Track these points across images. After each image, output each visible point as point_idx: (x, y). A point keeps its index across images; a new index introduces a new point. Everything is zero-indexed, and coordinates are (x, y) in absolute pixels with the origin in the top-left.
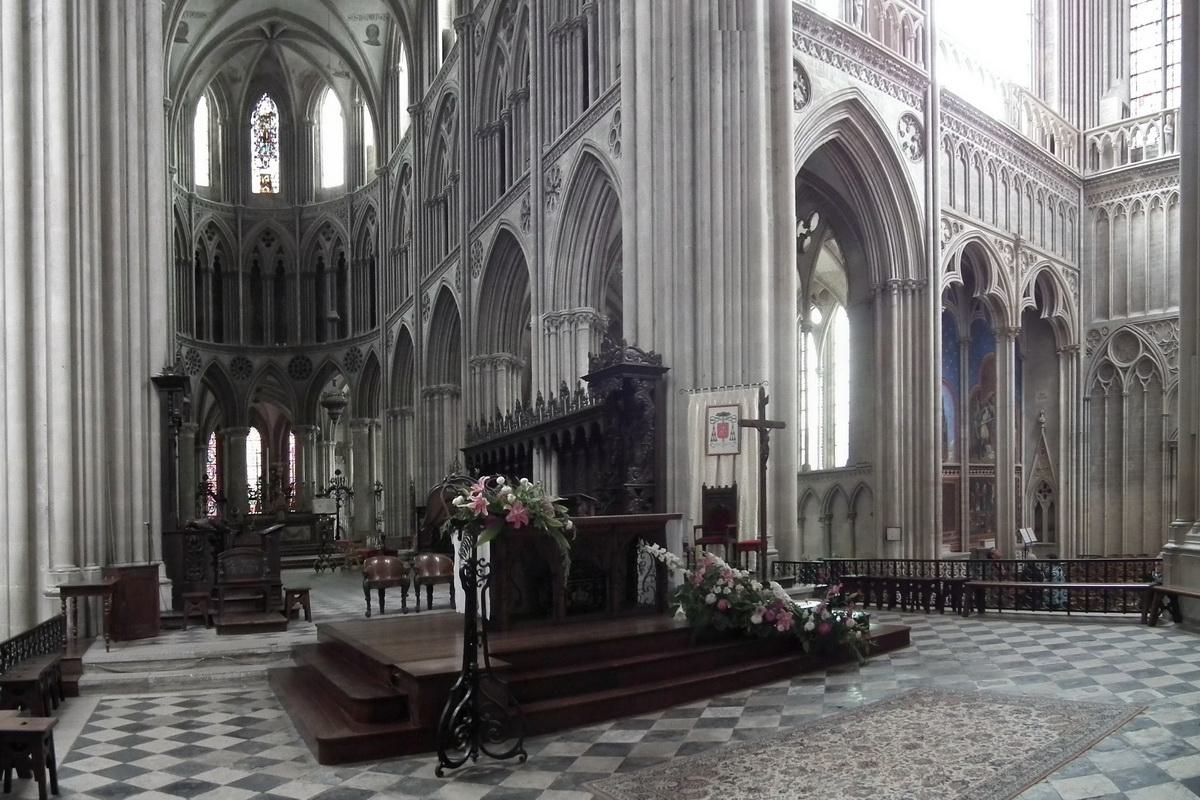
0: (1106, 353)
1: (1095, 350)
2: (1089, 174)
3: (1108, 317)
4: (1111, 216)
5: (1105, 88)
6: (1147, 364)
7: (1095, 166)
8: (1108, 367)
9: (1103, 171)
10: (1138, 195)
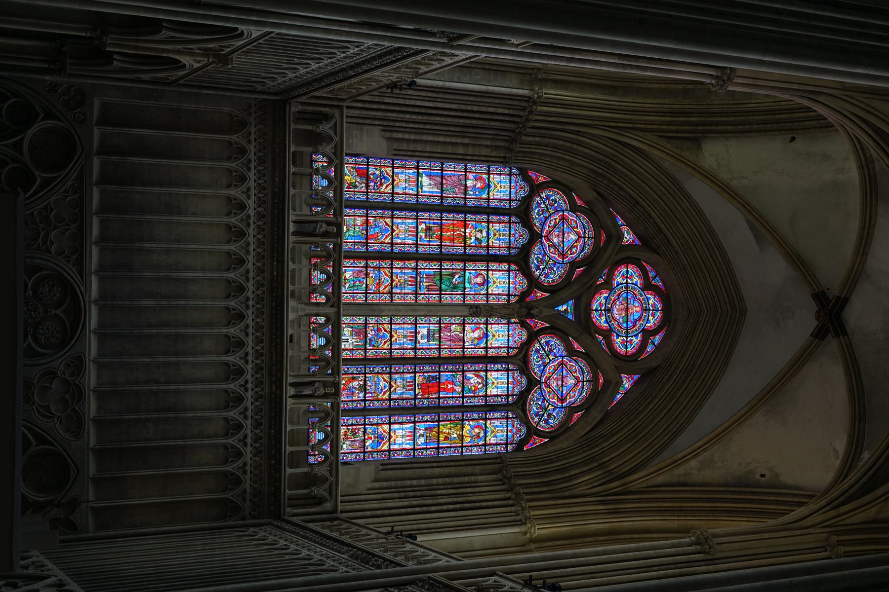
4: (234, 138)
7: (301, 117)
10: (252, 181)
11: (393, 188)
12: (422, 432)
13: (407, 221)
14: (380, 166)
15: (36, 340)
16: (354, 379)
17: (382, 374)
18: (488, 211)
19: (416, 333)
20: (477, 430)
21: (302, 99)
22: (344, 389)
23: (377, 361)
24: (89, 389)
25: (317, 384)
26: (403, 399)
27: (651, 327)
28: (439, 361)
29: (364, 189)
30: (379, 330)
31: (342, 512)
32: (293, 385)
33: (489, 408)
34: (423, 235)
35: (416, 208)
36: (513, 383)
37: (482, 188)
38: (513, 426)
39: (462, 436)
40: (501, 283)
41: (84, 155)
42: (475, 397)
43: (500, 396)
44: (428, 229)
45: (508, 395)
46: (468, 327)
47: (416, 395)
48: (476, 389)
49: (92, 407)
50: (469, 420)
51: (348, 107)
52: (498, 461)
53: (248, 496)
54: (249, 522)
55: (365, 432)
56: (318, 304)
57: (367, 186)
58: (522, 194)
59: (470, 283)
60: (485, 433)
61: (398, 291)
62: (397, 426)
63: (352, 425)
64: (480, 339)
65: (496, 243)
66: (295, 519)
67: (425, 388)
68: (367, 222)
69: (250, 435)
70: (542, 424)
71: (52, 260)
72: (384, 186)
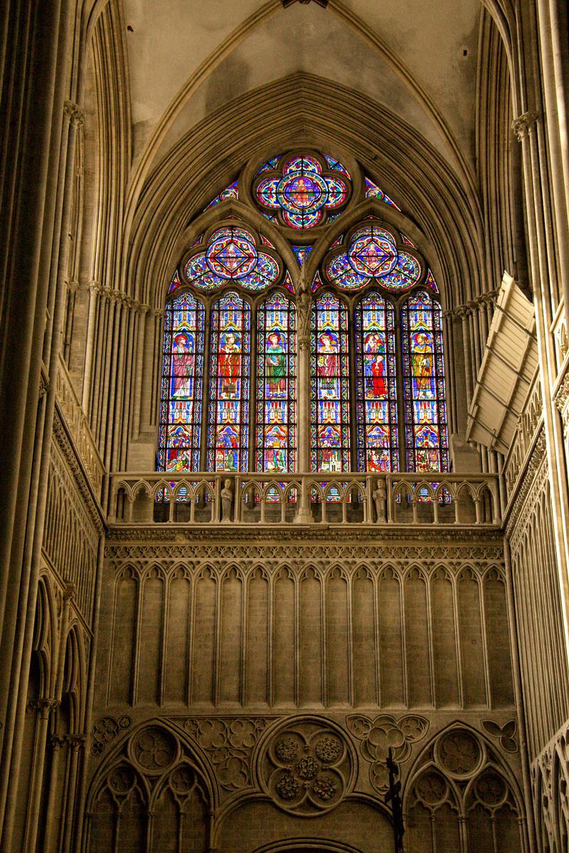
0: (124, 751)
1: (108, 747)
2: (112, 520)
3: (130, 701)
5: (136, 431)
6: (188, 773)
7: (121, 514)
8: (128, 772)
9: (131, 522)
10: (182, 560)
11: (187, 424)
12: (421, 393)
13: (219, 410)
14: (167, 437)
15: (333, 761)
16: (371, 460)
17: (365, 433)
18: (209, 329)
19: (326, 400)
20: (420, 340)
21: (104, 514)
22: (380, 469)
23: (353, 437)
24: (380, 711)
25: (375, 496)
26: (390, 412)
27: (319, 168)
28: (354, 378)
29: (189, 452)
30: (323, 436)
31: (497, 471)
32: (375, 520)
33: (400, 330)
34: (232, 395)
35: (207, 402)
36: (374, 305)
37: (186, 338)
38: (416, 305)
39: (425, 354)
40: (276, 320)
41: (160, 718)
42: (387, 343)
43: (386, 318)
44: (226, 390)
45: (386, 310)
46: (320, 350)
47: (385, 400)
48: (379, 341)
49: (398, 709)
50: (410, 348)
51: (111, 470)
52: (449, 319)
53: (481, 561)
54: (506, 559)
55: (421, 449)
56: (299, 496)
57: (186, 449)
58: (191, 300)
59: (276, 349)
60: (422, 331)
61: (286, 418)
62: (416, 418)
63: (414, 461)
64: (331, 338)
65: (239, 323)
66: (504, 516)
67: (378, 390)
68: (220, 449)
69: (423, 559)
70: (413, 276)
71: (259, 746)
72: (185, 432)
